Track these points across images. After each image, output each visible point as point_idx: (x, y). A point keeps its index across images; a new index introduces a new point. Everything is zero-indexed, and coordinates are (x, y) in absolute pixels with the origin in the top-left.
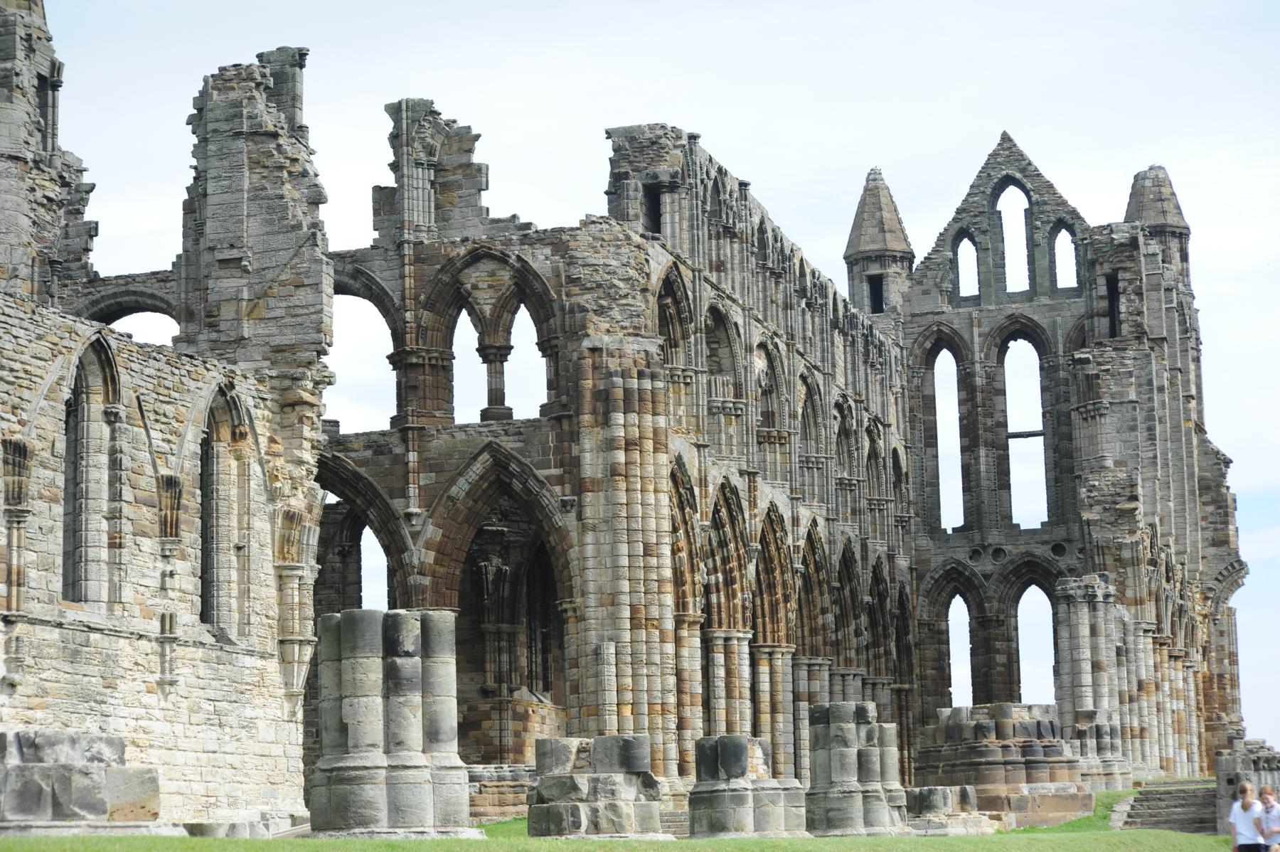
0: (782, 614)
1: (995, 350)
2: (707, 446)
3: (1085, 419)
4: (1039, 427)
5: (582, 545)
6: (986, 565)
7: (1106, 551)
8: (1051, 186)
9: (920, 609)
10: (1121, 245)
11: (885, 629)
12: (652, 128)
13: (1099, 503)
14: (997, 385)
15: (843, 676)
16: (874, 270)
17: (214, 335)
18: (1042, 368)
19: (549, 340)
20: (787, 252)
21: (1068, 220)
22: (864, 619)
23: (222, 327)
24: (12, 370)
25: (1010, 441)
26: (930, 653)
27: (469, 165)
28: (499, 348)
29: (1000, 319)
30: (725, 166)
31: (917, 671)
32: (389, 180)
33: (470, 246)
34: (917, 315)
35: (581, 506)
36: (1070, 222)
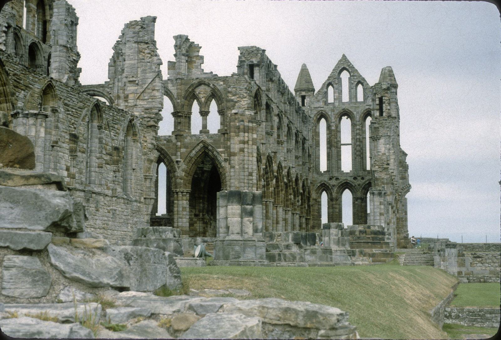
0: (281, 194)
2: (265, 144)
3: (374, 140)
4: (350, 142)
5: (230, 172)
8: (357, 71)
9: (314, 195)
10: (384, 89)
11: (304, 200)
12: (252, 47)
13: (377, 165)
16: (303, 93)
17: (126, 104)
18: (352, 125)
19: (222, 110)
20: (285, 87)
21: (362, 82)
22: (300, 197)
23: (130, 101)
24: (72, 112)
25: (342, 146)
27: (198, 56)
28: (206, 112)
29: (340, 110)
30: (271, 60)
31: (312, 213)
32: (173, 59)
33: (198, 80)
34: (316, 108)
35: (230, 160)
36: (362, 82)
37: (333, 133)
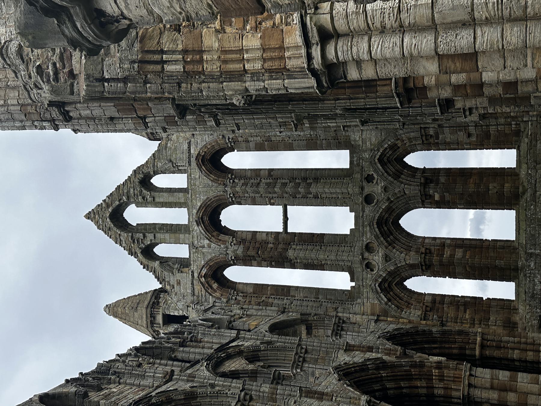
1: (222, 237)
6: (377, 259)
7: (152, 45)
8: (119, 187)
11: (414, 365)
14: (249, 236)
15: (470, 385)
16: (159, 319)
25: (289, 230)
26: (451, 313)
31: (466, 327)
37: (252, 252)
